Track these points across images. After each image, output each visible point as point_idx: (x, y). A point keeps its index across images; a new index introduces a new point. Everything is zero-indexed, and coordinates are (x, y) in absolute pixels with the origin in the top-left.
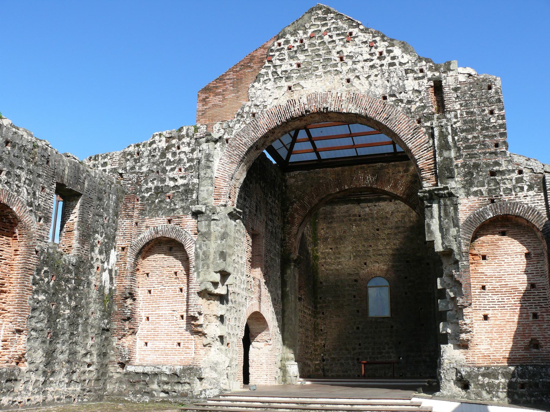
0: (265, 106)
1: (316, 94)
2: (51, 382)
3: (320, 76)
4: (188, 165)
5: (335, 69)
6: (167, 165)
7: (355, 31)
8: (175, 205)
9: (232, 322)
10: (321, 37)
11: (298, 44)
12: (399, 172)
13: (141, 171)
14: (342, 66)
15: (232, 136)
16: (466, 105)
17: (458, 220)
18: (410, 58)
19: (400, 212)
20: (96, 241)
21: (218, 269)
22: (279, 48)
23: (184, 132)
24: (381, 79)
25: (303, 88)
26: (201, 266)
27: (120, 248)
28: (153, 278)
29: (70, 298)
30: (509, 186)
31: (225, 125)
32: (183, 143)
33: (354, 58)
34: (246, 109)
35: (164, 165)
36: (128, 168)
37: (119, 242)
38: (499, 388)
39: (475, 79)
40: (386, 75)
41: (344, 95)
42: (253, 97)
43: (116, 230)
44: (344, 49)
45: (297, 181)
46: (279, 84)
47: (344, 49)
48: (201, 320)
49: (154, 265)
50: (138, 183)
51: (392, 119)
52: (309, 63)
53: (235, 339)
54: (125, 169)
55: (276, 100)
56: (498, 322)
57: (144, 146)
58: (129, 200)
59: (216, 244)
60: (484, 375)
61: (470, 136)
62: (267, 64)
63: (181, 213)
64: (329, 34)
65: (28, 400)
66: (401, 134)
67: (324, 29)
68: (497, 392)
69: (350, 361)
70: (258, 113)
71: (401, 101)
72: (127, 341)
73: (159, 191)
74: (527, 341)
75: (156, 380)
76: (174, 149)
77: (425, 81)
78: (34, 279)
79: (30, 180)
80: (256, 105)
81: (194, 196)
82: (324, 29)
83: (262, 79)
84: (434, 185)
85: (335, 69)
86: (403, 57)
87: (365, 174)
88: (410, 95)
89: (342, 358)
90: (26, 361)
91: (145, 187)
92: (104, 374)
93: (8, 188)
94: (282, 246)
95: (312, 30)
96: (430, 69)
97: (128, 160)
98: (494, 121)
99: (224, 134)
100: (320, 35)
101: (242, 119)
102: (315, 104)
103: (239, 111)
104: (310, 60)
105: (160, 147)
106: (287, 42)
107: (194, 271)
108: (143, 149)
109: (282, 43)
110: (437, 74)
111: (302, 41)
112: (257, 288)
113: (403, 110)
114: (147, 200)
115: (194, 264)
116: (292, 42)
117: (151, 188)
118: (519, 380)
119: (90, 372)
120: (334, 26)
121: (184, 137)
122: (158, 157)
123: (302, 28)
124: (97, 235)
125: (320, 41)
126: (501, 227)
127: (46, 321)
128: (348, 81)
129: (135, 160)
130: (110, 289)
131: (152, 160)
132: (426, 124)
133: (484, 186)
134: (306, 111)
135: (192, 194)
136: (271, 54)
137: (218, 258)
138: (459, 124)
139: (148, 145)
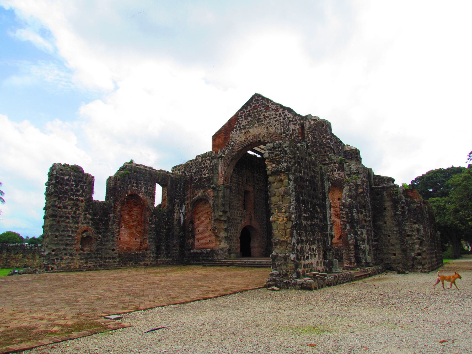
0: (236, 141)
1: (255, 135)
2: (159, 257)
3: (257, 127)
4: (209, 168)
6: (202, 168)
8: (205, 185)
11: (248, 113)
14: (265, 121)
16: (314, 134)
20: (176, 202)
25: (250, 133)
29: (165, 226)
31: (222, 150)
32: (207, 159)
34: (230, 143)
40: (282, 123)
41: (266, 134)
43: (184, 197)
47: (265, 113)
52: (252, 121)
55: (240, 139)
61: (314, 149)
62: (237, 123)
64: (260, 107)
65: (151, 263)
67: (258, 105)
71: (288, 135)
72: (191, 241)
73: (200, 179)
76: (204, 162)
78: (150, 220)
79: (145, 184)
80: (233, 141)
86: (289, 115)
93: (137, 188)
95: (253, 106)
96: (299, 120)
98: (324, 141)
103: (227, 144)
106: (244, 112)
110: (302, 121)
111: (249, 111)
113: (288, 139)
114: (196, 183)
116: (245, 112)
117: (197, 178)
119: (176, 253)
120: (261, 103)
122: (198, 166)
123: (249, 105)
124: (176, 200)
125: (256, 111)
127: (156, 235)
128: (267, 128)
130: (183, 220)
134: (252, 142)
135: (211, 180)
138: (310, 144)
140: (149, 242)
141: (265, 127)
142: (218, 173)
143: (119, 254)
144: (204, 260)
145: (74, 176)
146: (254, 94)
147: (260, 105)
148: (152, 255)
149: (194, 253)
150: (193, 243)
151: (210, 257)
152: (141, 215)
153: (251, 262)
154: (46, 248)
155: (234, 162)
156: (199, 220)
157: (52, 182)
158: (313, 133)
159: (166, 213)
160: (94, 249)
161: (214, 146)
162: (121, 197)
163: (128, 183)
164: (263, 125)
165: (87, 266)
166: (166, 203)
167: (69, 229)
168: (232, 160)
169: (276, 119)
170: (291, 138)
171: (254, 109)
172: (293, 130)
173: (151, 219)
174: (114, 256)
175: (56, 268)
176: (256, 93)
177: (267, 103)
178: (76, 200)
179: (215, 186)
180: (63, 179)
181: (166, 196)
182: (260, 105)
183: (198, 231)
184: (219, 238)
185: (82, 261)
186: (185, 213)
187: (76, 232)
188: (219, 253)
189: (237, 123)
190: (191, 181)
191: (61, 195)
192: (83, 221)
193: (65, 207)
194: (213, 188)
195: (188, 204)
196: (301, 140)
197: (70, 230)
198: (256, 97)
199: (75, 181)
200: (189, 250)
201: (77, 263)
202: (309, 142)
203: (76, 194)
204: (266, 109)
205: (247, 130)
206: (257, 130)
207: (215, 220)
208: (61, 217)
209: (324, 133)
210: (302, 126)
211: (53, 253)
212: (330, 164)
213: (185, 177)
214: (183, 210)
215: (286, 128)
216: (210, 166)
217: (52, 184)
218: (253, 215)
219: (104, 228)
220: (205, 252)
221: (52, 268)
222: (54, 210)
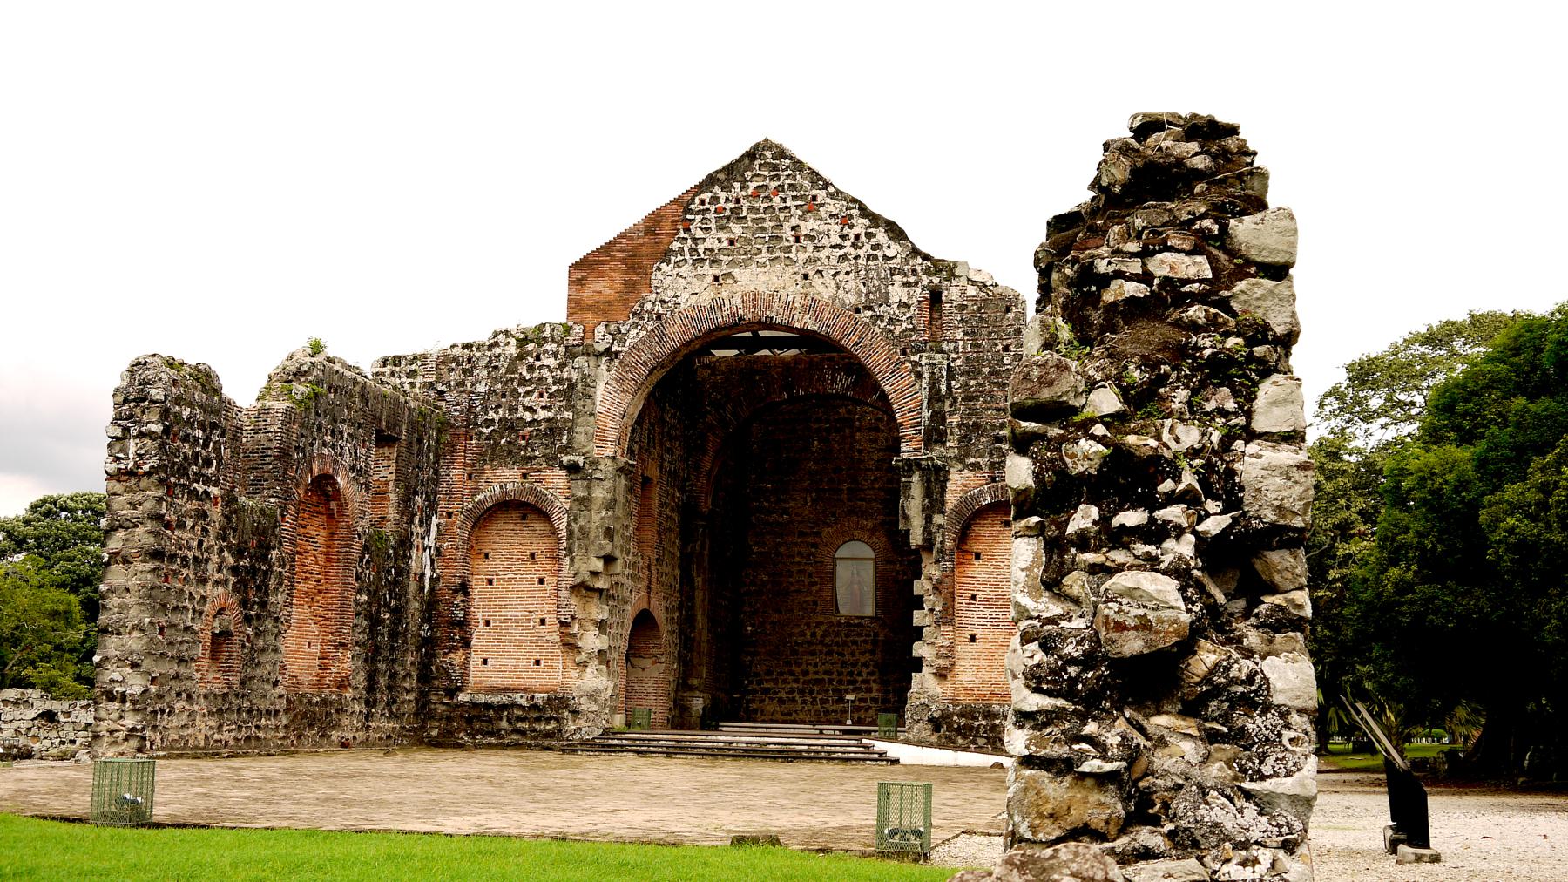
3: (764, 265)
4: (554, 388)
5: (787, 255)
7: (821, 194)
8: (533, 450)
9: (614, 631)
10: (769, 198)
11: (732, 205)
13: (476, 391)
14: (798, 251)
15: (625, 349)
16: (973, 332)
17: (943, 502)
18: (900, 250)
21: (602, 553)
23: (547, 334)
24: (855, 278)
28: (496, 563)
31: (613, 328)
32: (546, 351)
33: (816, 241)
34: (648, 306)
35: (515, 385)
36: (452, 383)
38: (978, 732)
39: (990, 294)
40: (863, 272)
41: (798, 299)
43: (436, 486)
45: (713, 374)
47: (802, 223)
48: (575, 629)
50: (471, 408)
51: (866, 346)
53: (615, 655)
54: (448, 384)
57: (478, 349)
58: (455, 435)
59: (599, 516)
60: (961, 715)
61: (973, 383)
62: (682, 234)
63: (544, 465)
64: (781, 194)
65: (354, 737)
67: (773, 184)
68: (975, 736)
69: (796, 695)
72: (457, 658)
73: (509, 426)
75: (506, 713)
77: (918, 290)
80: (663, 302)
82: (773, 184)
83: (673, 258)
84: (916, 450)
85: (787, 255)
86: (889, 247)
87: (835, 371)
89: (783, 689)
90: (350, 685)
91: (482, 417)
92: (424, 707)
94: (682, 491)
95: (755, 184)
96: (927, 272)
97: (453, 369)
100: (767, 194)
101: (641, 322)
106: (715, 199)
108: (478, 354)
109: (707, 201)
110: (936, 280)
111: (738, 201)
112: (646, 571)
116: (722, 201)
117: (493, 420)
119: (410, 701)
120: (789, 181)
123: (739, 178)
125: (766, 205)
128: (806, 276)
129: (465, 371)
130: (431, 578)
132: (912, 358)
133: (982, 457)
134: (740, 319)
135: (561, 435)
136: (689, 217)
137: (601, 537)
138: (958, 363)
139: (486, 348)
140: (353, 656)
142: (591, 414)
143: (288, 700)
144: (517, 731)
145: (201, 407)
146: (761, 139)
147: (780, 188)
148: (357, 708)
149: (475, 705)
150: (464, 666)
151: (548, 720)
152: (327, 555)
153: (751, 743)
154: (128, 670)
155: (658, 375)
156: (490, 582)
157: (144, 429)
159: (394, 549)
160: (235, 680)
161: (575, 306)
162: (297, 486)
163: (315, 434)
165: (221, 741)
166: (391, 510)
167: (187, 603)
168: (651, 372)
169: (841, 252)
170: (892, 332)
171: (755, 196)
172: (902, 305)
173: (360, 570)
174: (278, 707)
175: (158, 742)
176: (767, 140)
178: (204, 496)
179: (581, 461)
180: (178, 415)
181: (387, 483)
182: (780, 188)
183: (487, 623)
185: (212, 723)
186: (437, 549)
187: (201, 613)
188: (583, 707)
189: (682, 234)
190: (467, 426)
191: (173, 479)
192: (217, 576)
193: (181, 525)
194: (573, 469)
195: (449, 515)
196: (926, 342)
197: (190, 606)
199: (203, 427)
200: (452, 692)
201: (203, 728)
203: (203, 475)
204: (805, 207)
205: (724, 269)
207: (573, 588)
208: (172, 558)
210: (935, 298)
211: (153, 689)
213: (439, 408)
214: (431, 541)
216: (557, 381)
217: (141, 435)
218: (654, 572)
219: (258, 603)
220: (526, 704)
221: (152, 743)
222: (156, 534)
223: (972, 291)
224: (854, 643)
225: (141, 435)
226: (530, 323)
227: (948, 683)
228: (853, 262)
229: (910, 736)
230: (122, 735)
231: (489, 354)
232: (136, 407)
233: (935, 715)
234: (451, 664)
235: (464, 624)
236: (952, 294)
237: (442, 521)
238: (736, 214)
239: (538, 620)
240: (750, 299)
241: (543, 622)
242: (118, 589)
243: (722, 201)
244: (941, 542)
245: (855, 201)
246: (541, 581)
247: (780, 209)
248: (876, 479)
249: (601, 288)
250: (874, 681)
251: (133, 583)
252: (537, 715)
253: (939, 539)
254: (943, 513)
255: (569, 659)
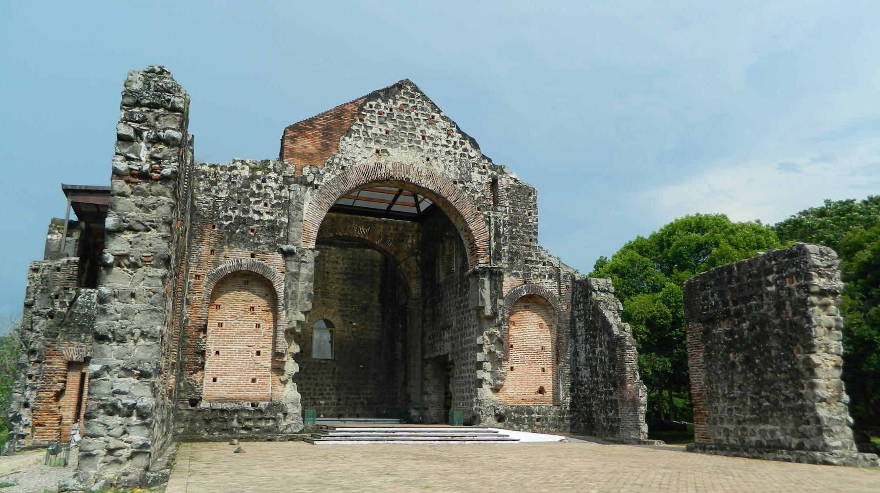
1: (401, 164)
3: (406, 149)
4: (275, 202)
5: (418, 145)
7: (437, 116)
8: (259, 239)
11: (388, 111)
12: (391, 229)
14: (424, 144)
16: (513, 203)
18: (477, 154)
19: (351, 259)
21: (306, 309)
22: (370, 109)
23: (271, 166)
24: (454, 165)
26: (289, 306)
27: (194, 276)
30: (537, 273)
32: (270, 178)
34: (336, 160)
35: (248, 196)
36: (201, 189)
37: (192, 269)
40: (458, 162)
41: (424, 171)
42: (343, 150)
44: (426, 130)
46: (368, 145)
47: (426, 130)
49: (227, 297)
50: (215, 207)
55: (364, 159)
56: (520, 373)
57: (221, 169)
58: (205, 223)
59: (304, 286)
60: (515, 412)
61: (514, 230)
62: (358, 122)
63: (266, 250)
64: (415, 111)
66: (466, 217)
67: (411, 105)
70: (348, 167)
72: (197, 377)
74: (537, 388)
75: (236, 416)
77: (486, 177)
80: (345, 159)
81: (282, 235)
82: (411, 105)
83: (353, 135)
85: (418, 145)
86: (471, 151)
88: (474, 185)
95: (402, 103)
96: (490, 167)
97: (202, 180)
99: (314, 179)
100: (407, 109)
101: (332, 169)
102: (398, 173)
103: (329, 160)
104: (397, 131)
105: (242, 174)
106: (378, 106)
107: (283, 310)
108: (221, 172)
109: (374, 106)
110: (495, 173)
111: (391, 110)
113: (468, 197)
114: (226, 228)
115: (283, 302)
116: (383, 108)
117: (231, 217)
118: (537, 415)
120: (420, 105)
121: (270, 172)
125: (407, 115)
126: (525, 302)
128: (428, 159)
131: (232, 187)
132: (484, 213)
133: (520, 270)
135: (279, 232)
136: (362, 113)
137: (306, 299)
138: (507, 218)
139: (227, 169)
141: (422, 156)
142: (301, 221)
144: (246, 428)
146: (404, 79)
147: (415, 108)
149: (213, 410)
156: (220, 325)
157: (161, 134)
158: (513, 201)
164: (418, 149)
169: (447, 150)
171: (401, 109)
177: (432, 111)
179: (294, 248)
182: (415, 108)
183: (217, 353)
184: (283, 374)
194: (287, 254)
198: (409, 87)
200: (194, 402)
202: (505, 215)
205: (384, 147)
206: (404, 156)
209: (530, 207)
210: (494, 183)
212: (538, 263)
215: (464, 175)
217: (158, 140)
220: (252, 409)
223: (512, 182)
224: (323, 373)
225: (157, 140)
226: (259, 159)
227: (500, 394)
228: (453, 156)
229: (486, 424)
230: (126, 453)
231: (229, 173)
232: (148, 111)
233: (502, 412)
234: (195, 382)
235: (203, 353)
236: (503, 182)
237: (191, 281)
238: (390, 116)
239: (255, 352)
240: (397, 166)
241: (258, 353)
242: (122, 294)
243: (383, 108)
244: (502, 315)
245: (454, 123)
246: (258, 326)
247: (415, 119)
248: (336, 287)
249: (307, 144)
250: (333, 394)
251: (140, 288)
252: (260, 416)
253: (500, 313)
254: (502, 298)
255: (276, 378)
